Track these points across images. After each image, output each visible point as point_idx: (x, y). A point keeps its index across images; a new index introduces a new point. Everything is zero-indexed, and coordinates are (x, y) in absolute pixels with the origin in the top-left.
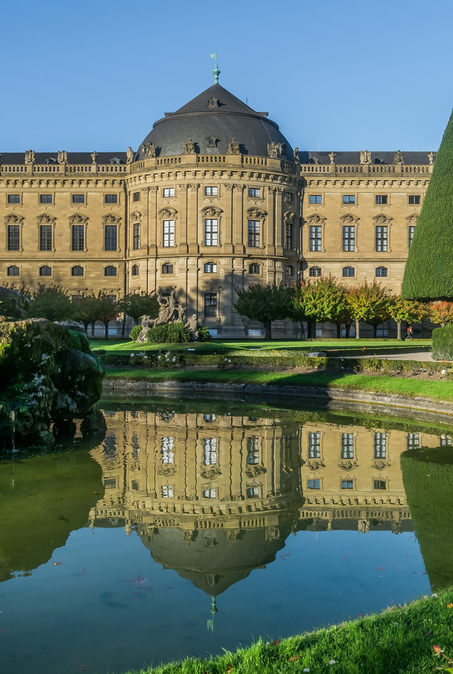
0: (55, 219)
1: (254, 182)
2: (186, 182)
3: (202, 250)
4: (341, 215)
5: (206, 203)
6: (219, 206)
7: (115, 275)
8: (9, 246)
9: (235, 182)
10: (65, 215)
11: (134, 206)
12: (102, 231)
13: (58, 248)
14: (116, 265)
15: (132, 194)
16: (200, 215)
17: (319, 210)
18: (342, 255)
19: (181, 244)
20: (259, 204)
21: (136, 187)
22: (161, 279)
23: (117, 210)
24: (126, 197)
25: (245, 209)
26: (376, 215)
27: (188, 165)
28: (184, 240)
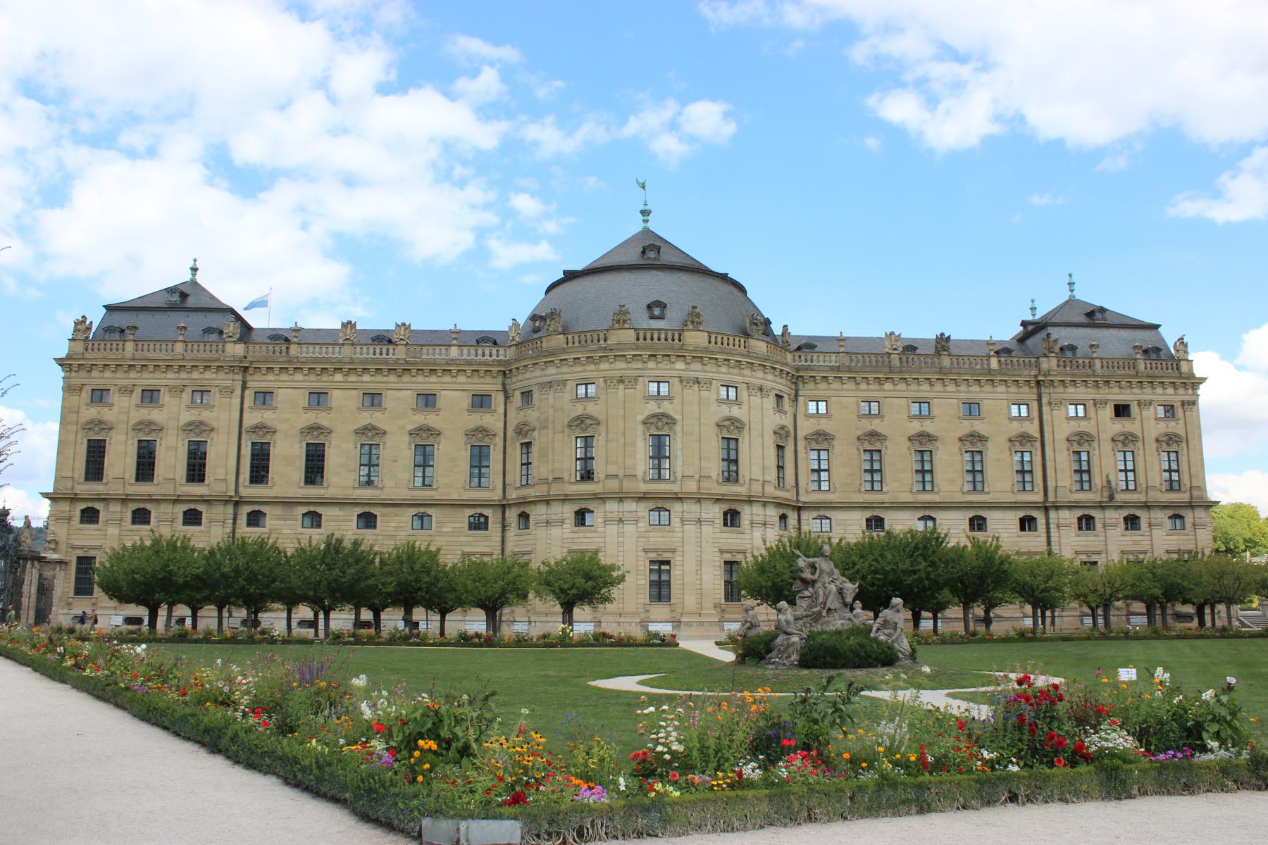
0: (385, 433)
1: (725, 374)
2: (618, 374)
3: (643, 487)
4: (859, 433)
5: (652, 408)
6: (671, 413)
7: (486, 528)
8: (306, 477)
9: (698, 374)
10: (403, 427)
11: (522, 413)
12: (465, 455)
13: (389, 483)
14: (487, 512)
15: (518, 394)
16: (640, 428)
17: (825, 425)
18: (860, 498)
19: (608, 476)
20: (735, 412)
21: (526, 383)
22: (572, 535)
23: (492, 421)
24: (507, 398)
25: (716, 418)
26: (912, 433)
27: (621, 346)
28: (612, 470)
